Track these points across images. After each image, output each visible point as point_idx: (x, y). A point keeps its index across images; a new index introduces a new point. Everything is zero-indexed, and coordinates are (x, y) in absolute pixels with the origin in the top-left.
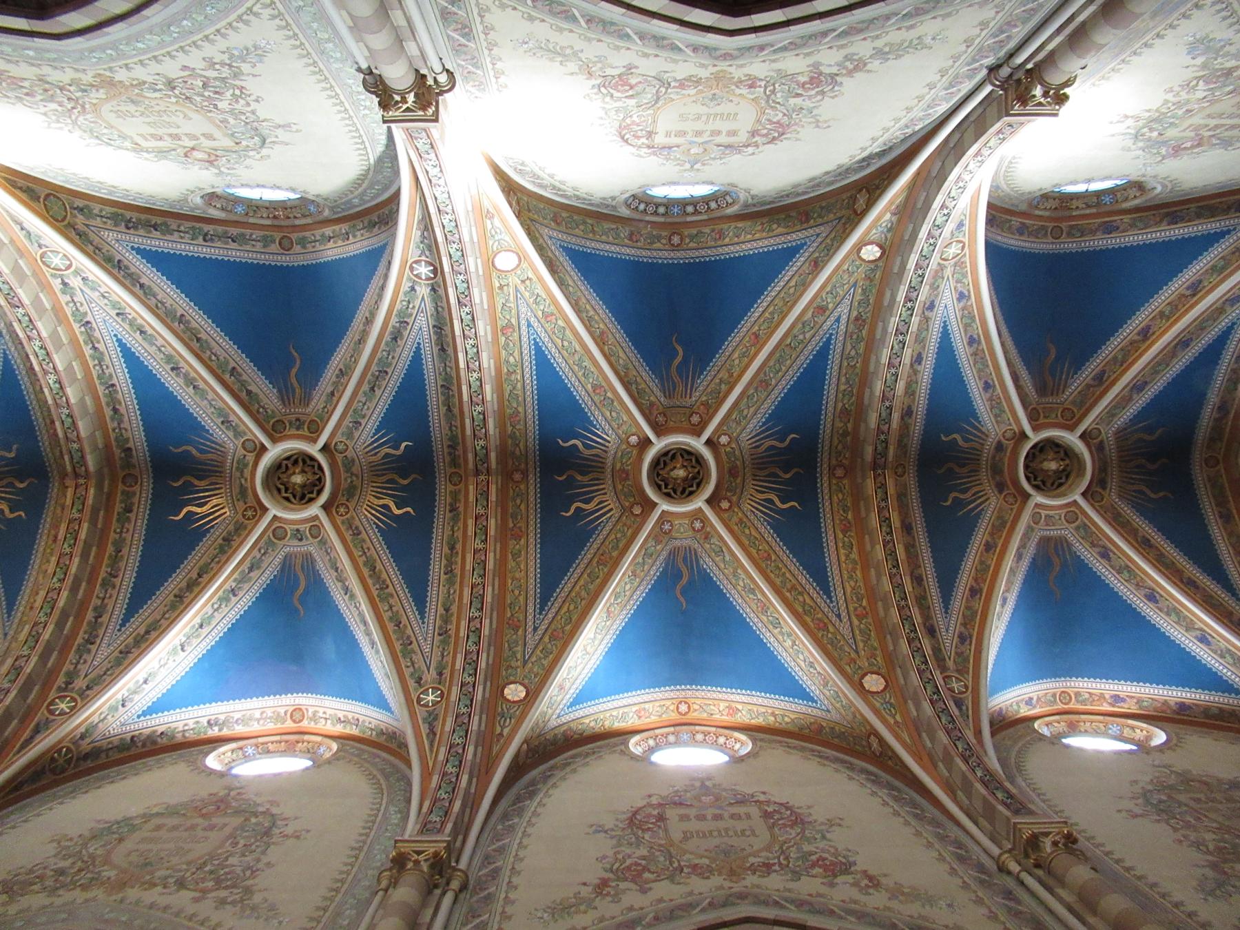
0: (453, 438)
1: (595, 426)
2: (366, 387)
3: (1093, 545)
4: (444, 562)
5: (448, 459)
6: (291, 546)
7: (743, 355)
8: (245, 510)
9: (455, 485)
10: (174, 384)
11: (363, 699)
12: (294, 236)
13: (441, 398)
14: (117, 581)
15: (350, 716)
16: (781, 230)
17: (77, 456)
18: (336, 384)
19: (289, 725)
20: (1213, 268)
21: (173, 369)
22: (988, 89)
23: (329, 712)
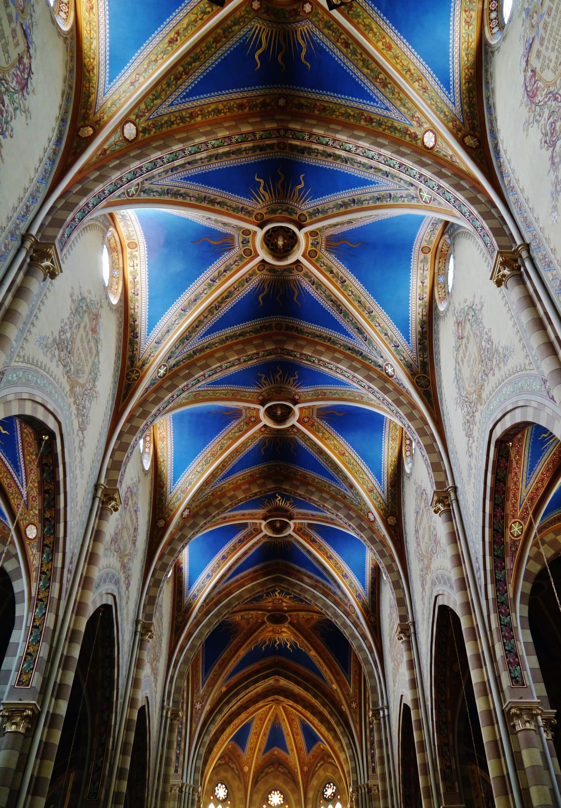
0: (301, 332)
1: (311, 200)
2: (333, 298)
3: (244, 537)
4: (232, 334)
5: (291, 325)
6: (238, 238)
7: (335, 446)
8: (261, 214)
9: (275, 326)
10: (345, 195)
11: (151, 299)
12: (429, 256)
13: (324, 335)
14: (214, 161)
15: (138, 286)
16: (390, 471)
17: (298, 134)
18: (336, 276)
19: (126, 242)
20: (351, 583)
21: (354, 200)
22: (519, 242)
23: (138, 268)
